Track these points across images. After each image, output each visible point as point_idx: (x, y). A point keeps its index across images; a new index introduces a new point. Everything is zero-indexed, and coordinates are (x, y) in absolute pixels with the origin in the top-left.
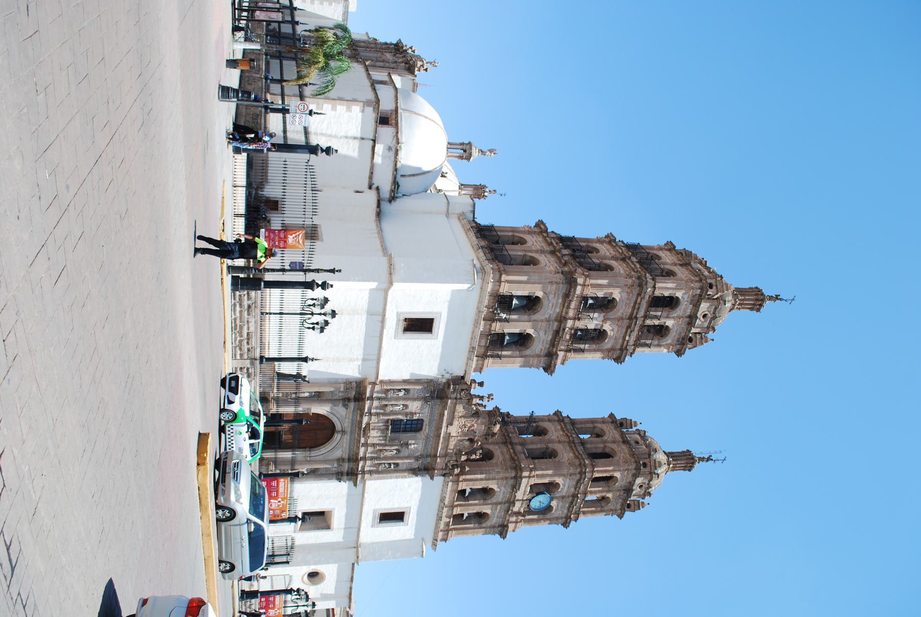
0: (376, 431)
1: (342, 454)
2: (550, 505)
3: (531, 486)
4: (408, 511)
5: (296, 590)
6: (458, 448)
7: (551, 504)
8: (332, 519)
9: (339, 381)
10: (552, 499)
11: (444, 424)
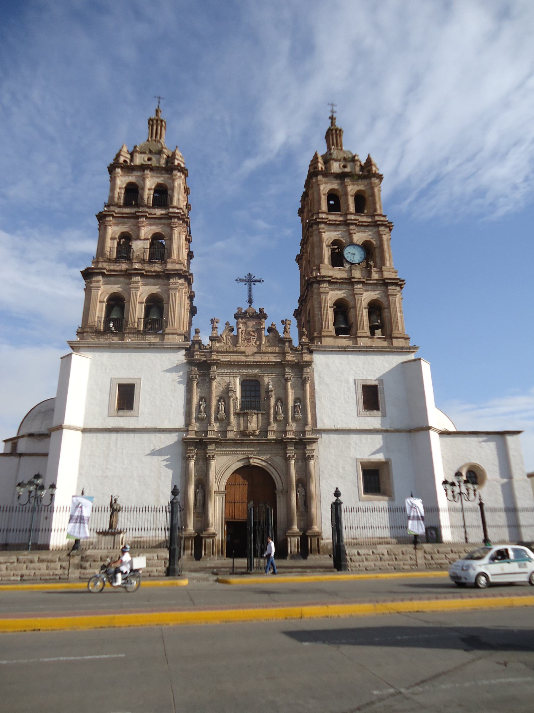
0: (249, 425)
1: (280, 456)
2: (362, 244)
3: (333, 267)
4: (361, 381)
5: (336, 498)
6: (277, 342)
7: (360, 244)
8: (372, 461)
9: (185, 465)
10: (352, 244)
11: (243, 358)
